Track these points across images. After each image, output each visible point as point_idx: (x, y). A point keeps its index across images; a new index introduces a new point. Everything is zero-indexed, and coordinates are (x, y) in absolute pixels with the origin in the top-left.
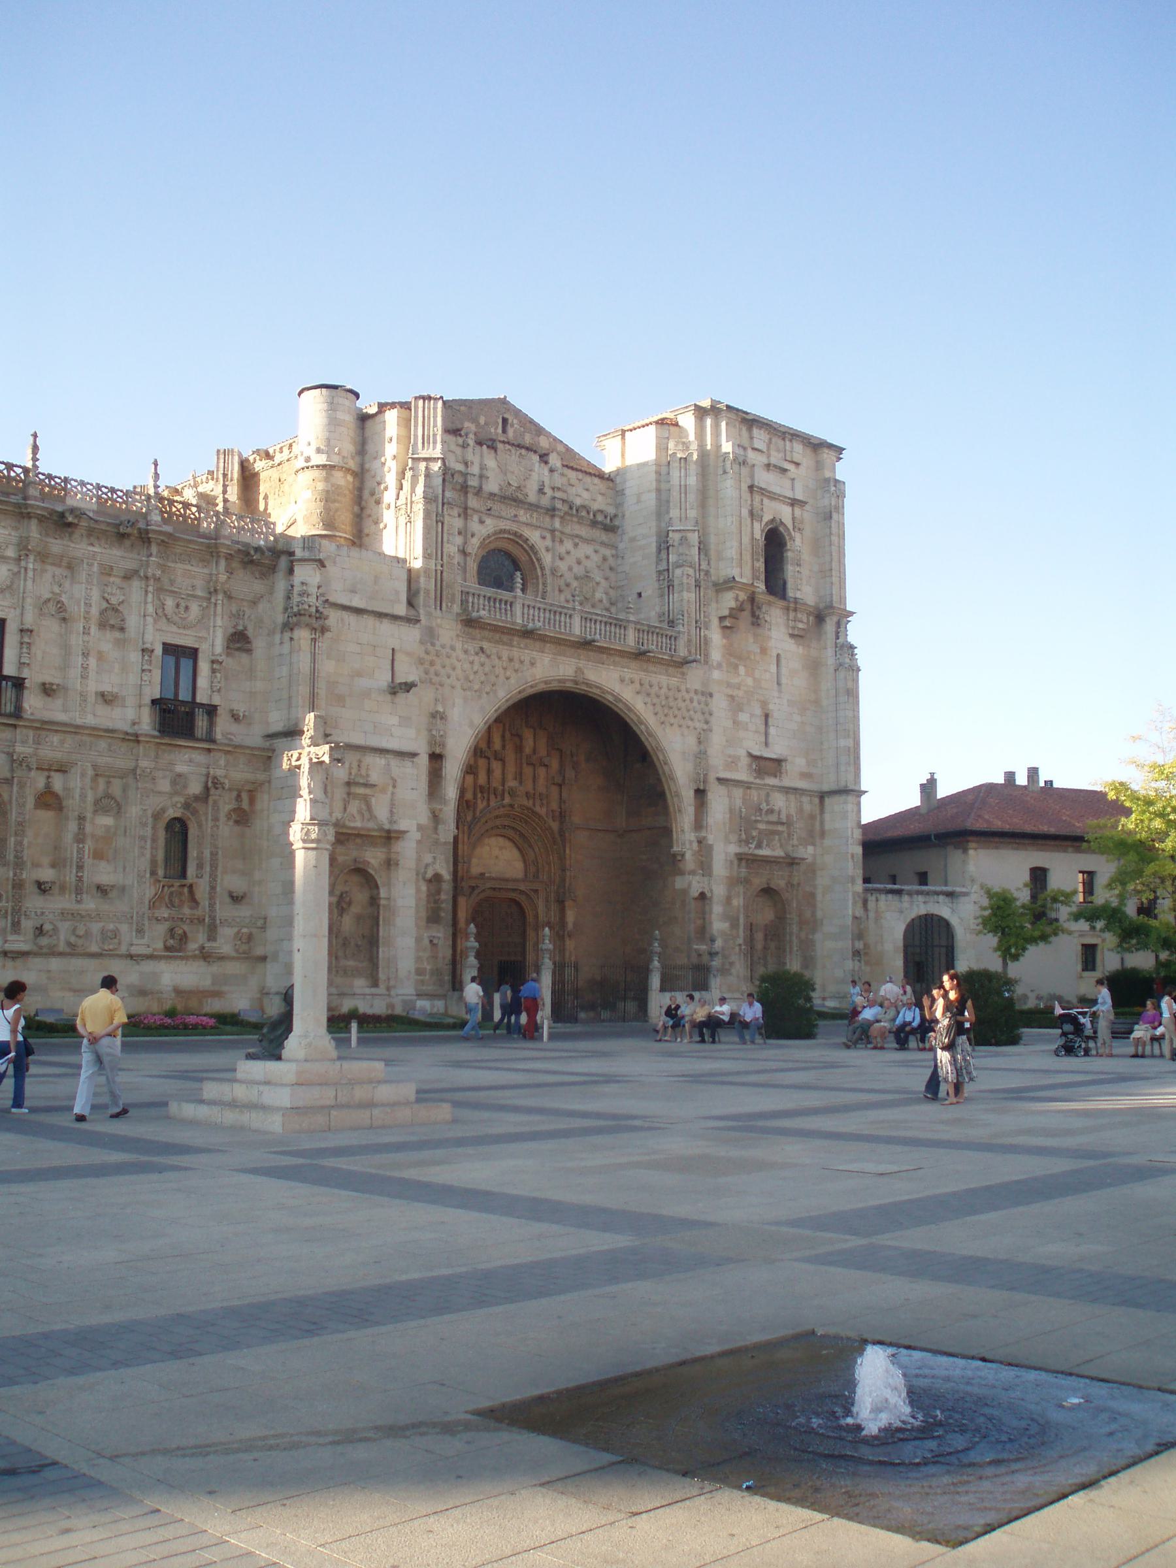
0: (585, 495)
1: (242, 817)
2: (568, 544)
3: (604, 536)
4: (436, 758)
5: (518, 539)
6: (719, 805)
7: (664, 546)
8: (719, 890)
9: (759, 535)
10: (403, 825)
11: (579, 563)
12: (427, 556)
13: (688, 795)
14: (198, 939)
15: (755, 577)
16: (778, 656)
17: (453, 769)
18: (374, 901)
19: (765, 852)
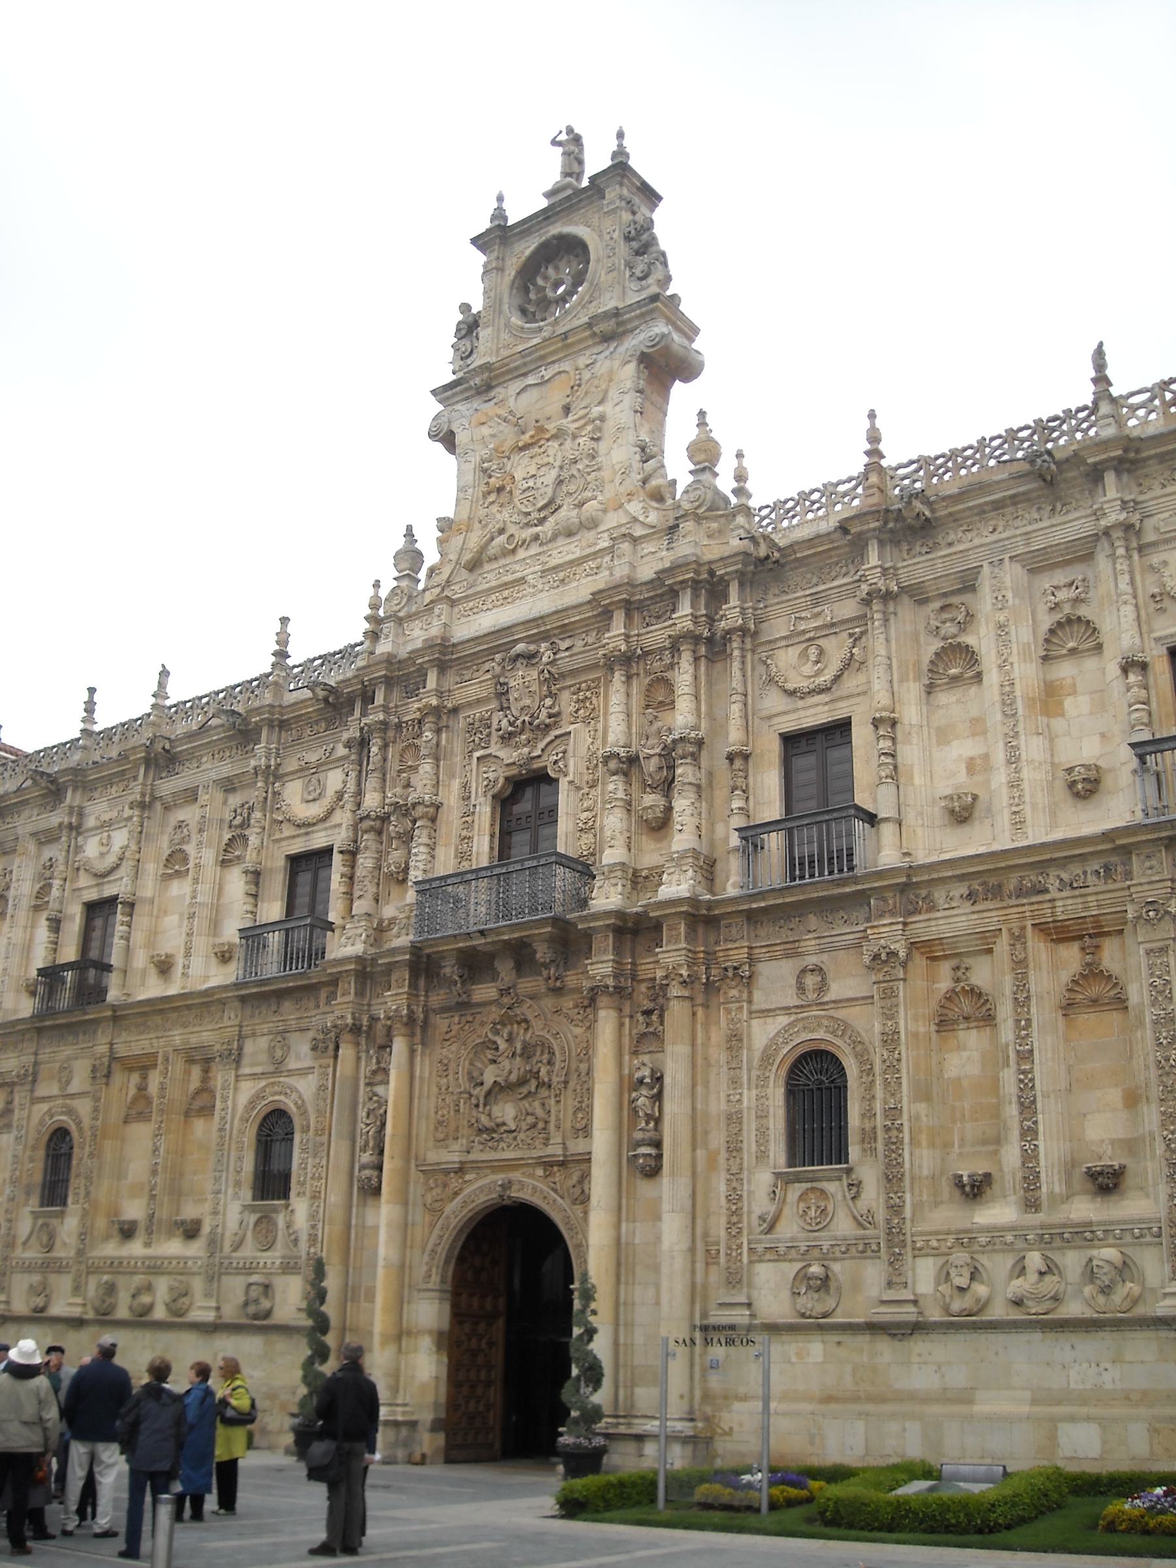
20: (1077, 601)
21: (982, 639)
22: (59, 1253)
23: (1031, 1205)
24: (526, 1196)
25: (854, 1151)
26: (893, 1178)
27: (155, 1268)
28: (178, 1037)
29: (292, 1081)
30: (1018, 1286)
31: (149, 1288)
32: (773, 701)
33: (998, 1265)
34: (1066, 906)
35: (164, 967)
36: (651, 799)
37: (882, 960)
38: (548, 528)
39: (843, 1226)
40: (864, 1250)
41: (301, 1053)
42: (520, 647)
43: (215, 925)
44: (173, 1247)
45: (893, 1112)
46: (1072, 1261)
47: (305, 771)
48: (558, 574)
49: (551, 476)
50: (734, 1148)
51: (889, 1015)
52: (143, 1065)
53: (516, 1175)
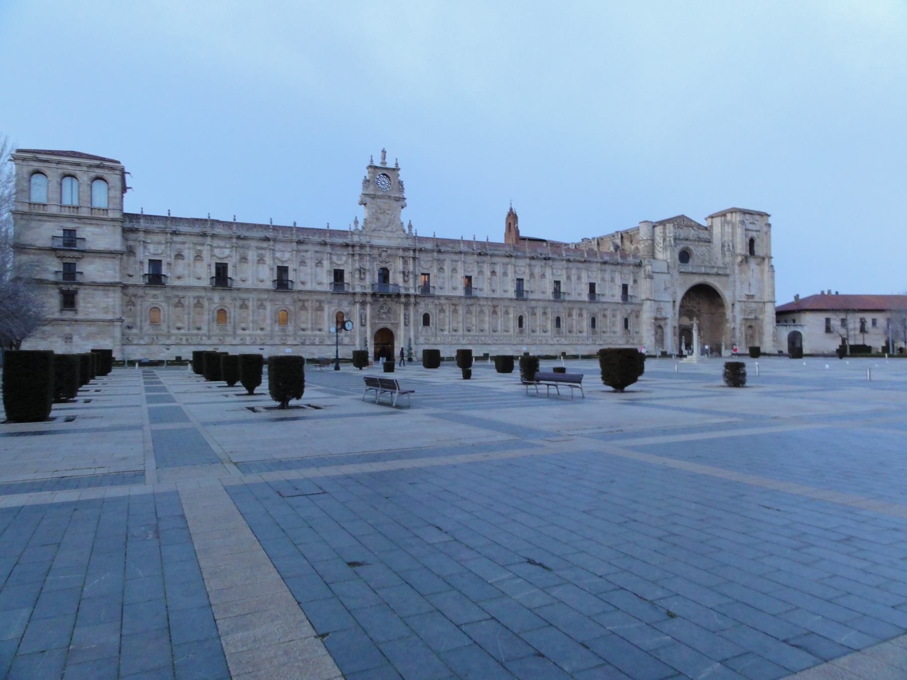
0: (703, 235)
1: (637, 317)
2: (699, 248)
3: (707, 244)
4: (674, 302)
5: (687, 248)
6: (738, 307)
7: (723, 246)
8: (738, 326)
9: (748, 241)
10: (668, 316)
11: (702, 251)
12: (671, 258)
13: (730, 305)
14: (631, 341)
15: (747, 251)
16: (753, 270)
17: (678, 304)
18: (663, 332)
19: (750, 317)
20: (456, 267)
21: (446, 268)
22: (288, 333)
23: (449, 332)
24: (388, 327)
25: (431, 325)
26: (436, 328)
27: (315, 336)
28: (316, 297)
29: (344, 308)
30: (448, 340)
31: (315, 339)
32: (421, 268)
33: (446, 338)
34: (455, 302)
35: (303, 283)
36: (406, 278)
37: (436, 305)
38: (387, 229)
39: (430, 333)
40: (432, 336)
41: (345, 303)
42: (385, 249)
43: (316, 277)
44: (318, 333)
45: (436, 321)
46: (453, 338)
47: (336, 254)
48: (389, 238)
49: (388, 221)
50: (418, 323)
51: (436, 310)
52: (304, 301)
53: (387, 325)
